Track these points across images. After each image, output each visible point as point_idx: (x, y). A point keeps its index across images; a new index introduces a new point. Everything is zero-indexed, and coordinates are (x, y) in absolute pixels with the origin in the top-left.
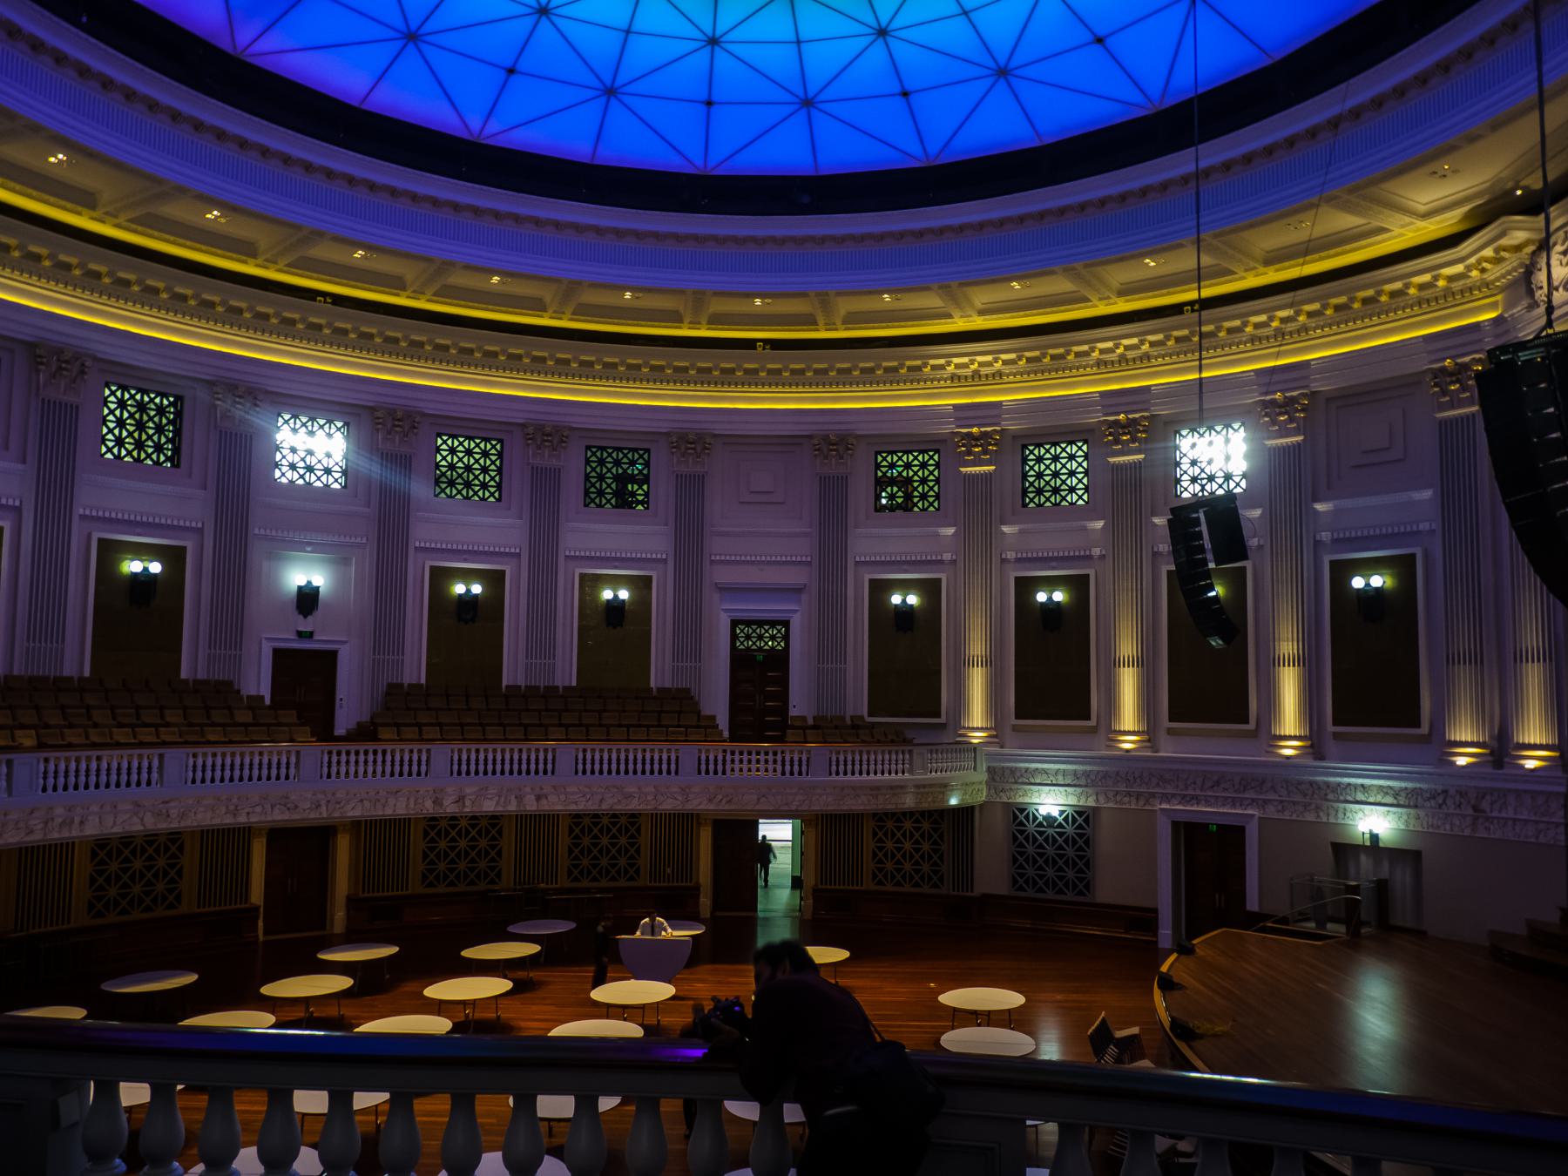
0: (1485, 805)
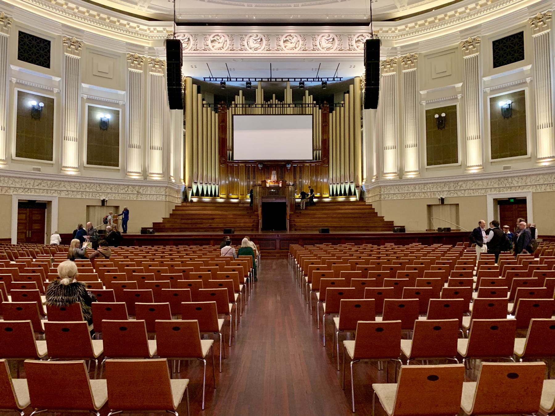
0: (141, 191)
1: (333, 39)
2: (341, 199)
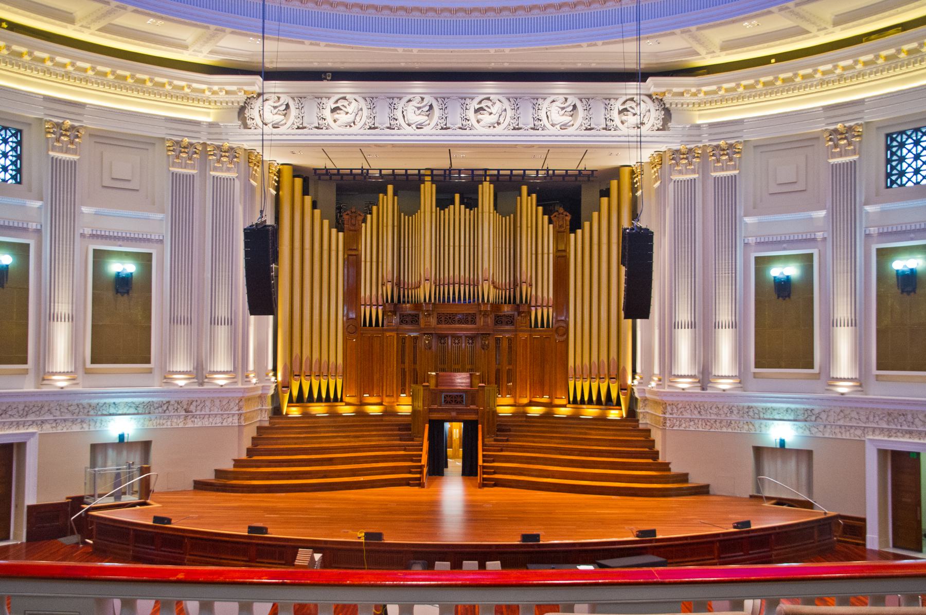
0: (192, 408)
1: (575, 107)
2: (590, 412)
